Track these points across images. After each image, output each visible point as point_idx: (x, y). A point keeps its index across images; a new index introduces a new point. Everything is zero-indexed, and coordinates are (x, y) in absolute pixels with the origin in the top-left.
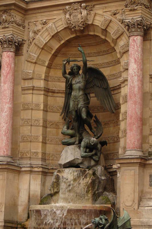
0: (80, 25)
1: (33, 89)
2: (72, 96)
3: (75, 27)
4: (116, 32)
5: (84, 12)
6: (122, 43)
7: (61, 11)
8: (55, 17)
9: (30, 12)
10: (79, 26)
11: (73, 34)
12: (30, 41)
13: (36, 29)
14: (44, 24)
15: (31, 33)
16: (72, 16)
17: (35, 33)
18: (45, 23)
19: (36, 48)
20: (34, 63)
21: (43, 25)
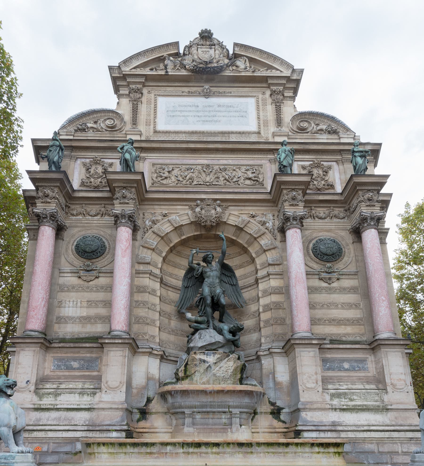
0: (213, 220)
1: (150, 274)
2: (205, 282)
3: (206, 221)
4: (256, 231)
5: (219, 209)
6: (264, 242)
7: (187, 207)
8: (178, 212)
9: (146, 203)
10: (211, 221)
11: (198, 231)
12: (146, 229)
13: (153, 218)
14: (164, 216)
15: (147, 222)
16: (203, 211)
17: (154, 222)
18: (165, 216)
19: (154, 236)
20: (151, 249)
21: (163, 217)
